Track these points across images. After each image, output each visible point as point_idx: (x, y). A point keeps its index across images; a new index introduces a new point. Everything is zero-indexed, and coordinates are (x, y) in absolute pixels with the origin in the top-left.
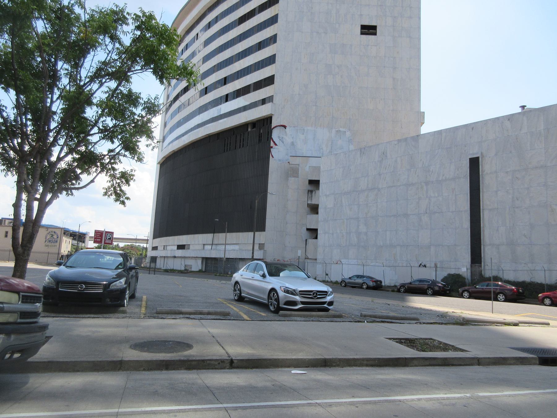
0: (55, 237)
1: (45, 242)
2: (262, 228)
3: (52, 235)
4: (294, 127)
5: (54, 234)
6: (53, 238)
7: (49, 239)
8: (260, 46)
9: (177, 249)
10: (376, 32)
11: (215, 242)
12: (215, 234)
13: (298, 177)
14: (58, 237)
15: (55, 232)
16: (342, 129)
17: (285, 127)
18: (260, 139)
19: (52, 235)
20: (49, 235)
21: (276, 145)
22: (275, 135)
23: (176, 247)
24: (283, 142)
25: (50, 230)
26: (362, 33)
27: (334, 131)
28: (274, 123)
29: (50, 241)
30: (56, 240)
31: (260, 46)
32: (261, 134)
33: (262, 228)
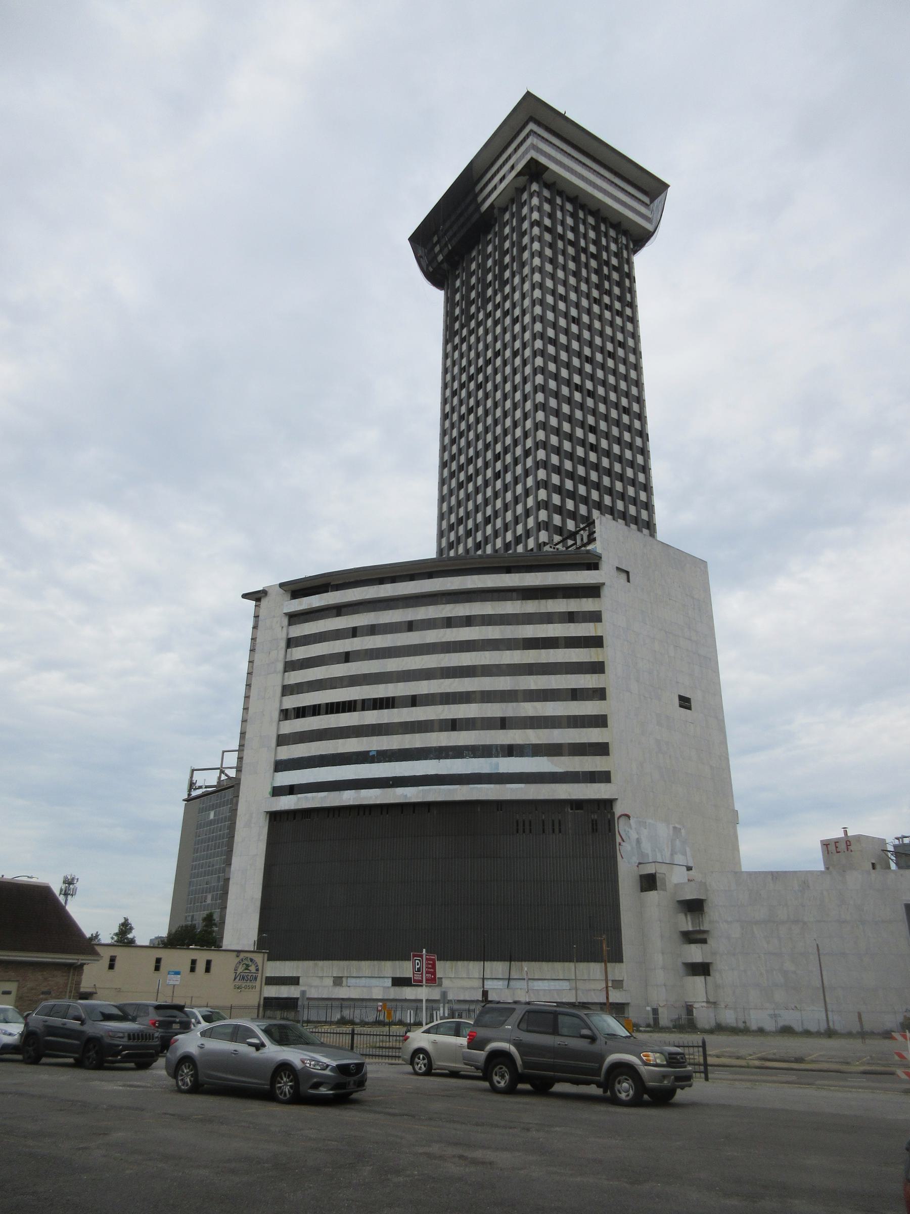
0: (253, 969)
1: (234, 980)
2: (617, 956)
3: (248, 966)
4: (637, 818)
5: (250, 963)
6: (248, 971)
7: (242, 974)
8: (575, 694)
9: (392, 985)
10: (691, 706)
11: (514, 975)
12: (513, 963)
13: (665, 890)
14: (257, 970)
15: (251, 960)
16: (677, 826)
17: (628, 816)
18: (595, 827)
19: (248, 966)
20: (241, 965)
21: (624, 841)
22: (621, 827)
23: (390, 980)
24: (629, 837)
25: (242, 955)
26: (681, 706)
27: (671, 826)
28: (618, 810)
29: (243, 978)
30: (254, 975)
31: (575, 694)
32: (596, 821)
33: (617, 956)
